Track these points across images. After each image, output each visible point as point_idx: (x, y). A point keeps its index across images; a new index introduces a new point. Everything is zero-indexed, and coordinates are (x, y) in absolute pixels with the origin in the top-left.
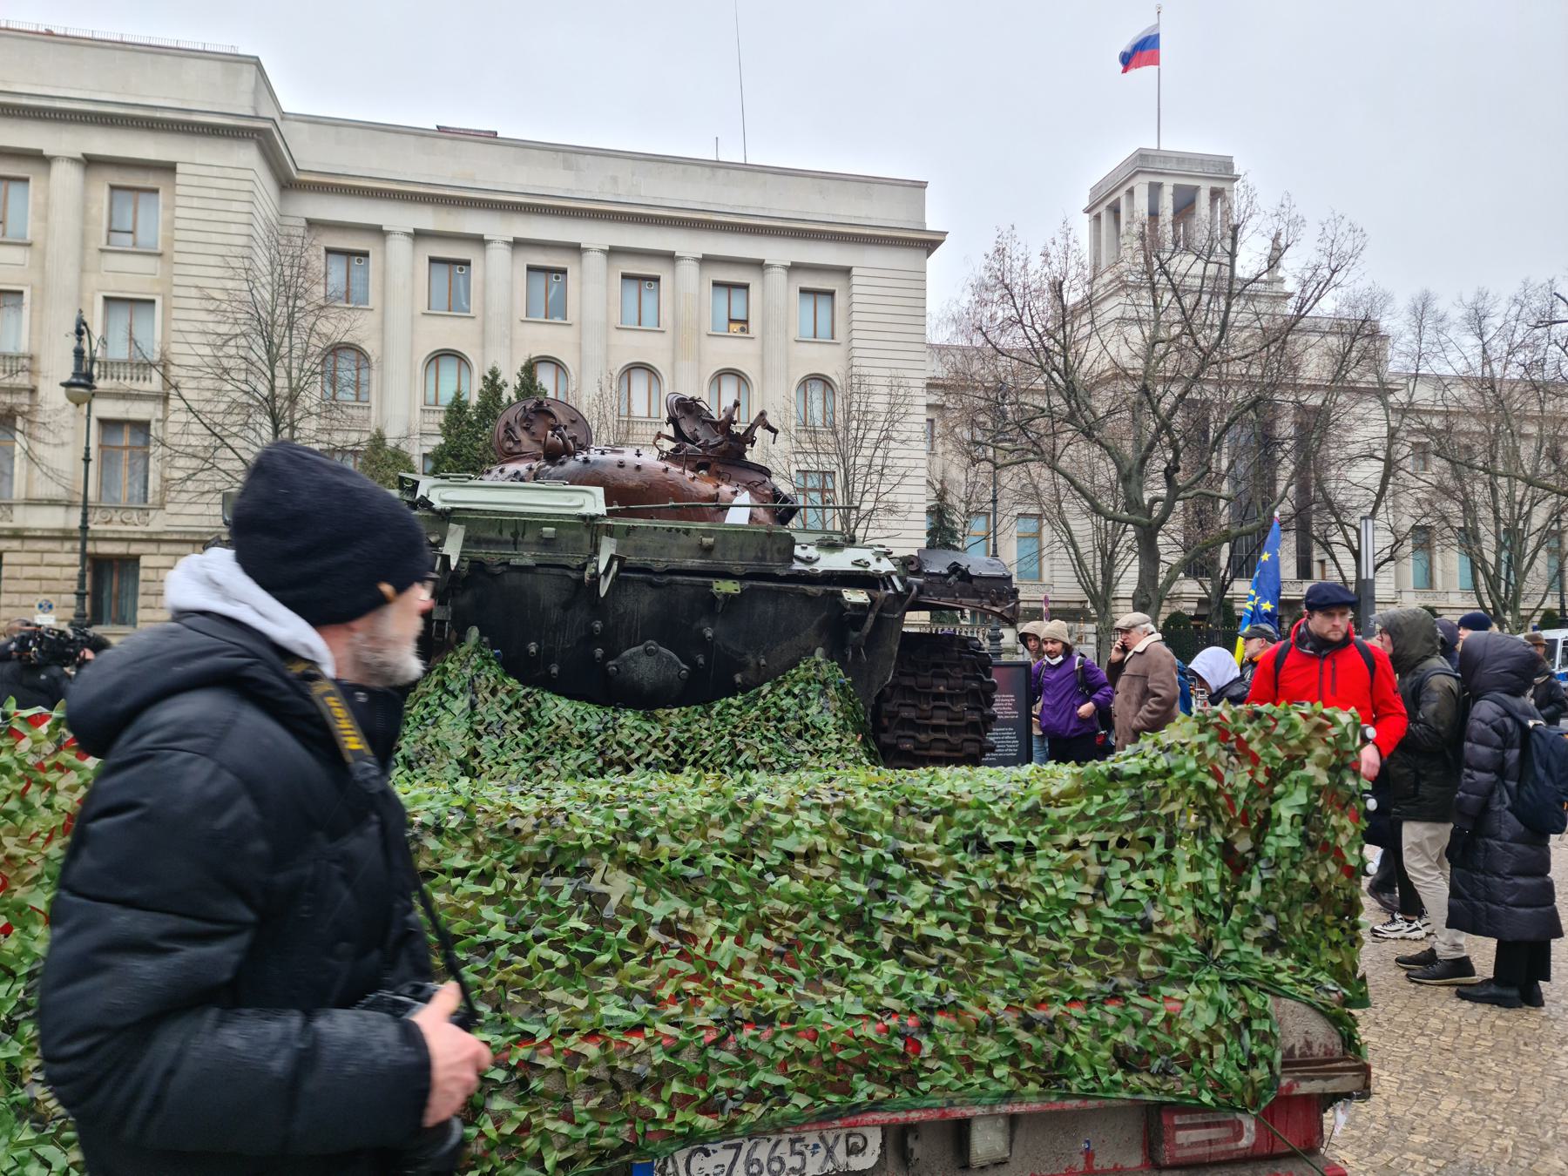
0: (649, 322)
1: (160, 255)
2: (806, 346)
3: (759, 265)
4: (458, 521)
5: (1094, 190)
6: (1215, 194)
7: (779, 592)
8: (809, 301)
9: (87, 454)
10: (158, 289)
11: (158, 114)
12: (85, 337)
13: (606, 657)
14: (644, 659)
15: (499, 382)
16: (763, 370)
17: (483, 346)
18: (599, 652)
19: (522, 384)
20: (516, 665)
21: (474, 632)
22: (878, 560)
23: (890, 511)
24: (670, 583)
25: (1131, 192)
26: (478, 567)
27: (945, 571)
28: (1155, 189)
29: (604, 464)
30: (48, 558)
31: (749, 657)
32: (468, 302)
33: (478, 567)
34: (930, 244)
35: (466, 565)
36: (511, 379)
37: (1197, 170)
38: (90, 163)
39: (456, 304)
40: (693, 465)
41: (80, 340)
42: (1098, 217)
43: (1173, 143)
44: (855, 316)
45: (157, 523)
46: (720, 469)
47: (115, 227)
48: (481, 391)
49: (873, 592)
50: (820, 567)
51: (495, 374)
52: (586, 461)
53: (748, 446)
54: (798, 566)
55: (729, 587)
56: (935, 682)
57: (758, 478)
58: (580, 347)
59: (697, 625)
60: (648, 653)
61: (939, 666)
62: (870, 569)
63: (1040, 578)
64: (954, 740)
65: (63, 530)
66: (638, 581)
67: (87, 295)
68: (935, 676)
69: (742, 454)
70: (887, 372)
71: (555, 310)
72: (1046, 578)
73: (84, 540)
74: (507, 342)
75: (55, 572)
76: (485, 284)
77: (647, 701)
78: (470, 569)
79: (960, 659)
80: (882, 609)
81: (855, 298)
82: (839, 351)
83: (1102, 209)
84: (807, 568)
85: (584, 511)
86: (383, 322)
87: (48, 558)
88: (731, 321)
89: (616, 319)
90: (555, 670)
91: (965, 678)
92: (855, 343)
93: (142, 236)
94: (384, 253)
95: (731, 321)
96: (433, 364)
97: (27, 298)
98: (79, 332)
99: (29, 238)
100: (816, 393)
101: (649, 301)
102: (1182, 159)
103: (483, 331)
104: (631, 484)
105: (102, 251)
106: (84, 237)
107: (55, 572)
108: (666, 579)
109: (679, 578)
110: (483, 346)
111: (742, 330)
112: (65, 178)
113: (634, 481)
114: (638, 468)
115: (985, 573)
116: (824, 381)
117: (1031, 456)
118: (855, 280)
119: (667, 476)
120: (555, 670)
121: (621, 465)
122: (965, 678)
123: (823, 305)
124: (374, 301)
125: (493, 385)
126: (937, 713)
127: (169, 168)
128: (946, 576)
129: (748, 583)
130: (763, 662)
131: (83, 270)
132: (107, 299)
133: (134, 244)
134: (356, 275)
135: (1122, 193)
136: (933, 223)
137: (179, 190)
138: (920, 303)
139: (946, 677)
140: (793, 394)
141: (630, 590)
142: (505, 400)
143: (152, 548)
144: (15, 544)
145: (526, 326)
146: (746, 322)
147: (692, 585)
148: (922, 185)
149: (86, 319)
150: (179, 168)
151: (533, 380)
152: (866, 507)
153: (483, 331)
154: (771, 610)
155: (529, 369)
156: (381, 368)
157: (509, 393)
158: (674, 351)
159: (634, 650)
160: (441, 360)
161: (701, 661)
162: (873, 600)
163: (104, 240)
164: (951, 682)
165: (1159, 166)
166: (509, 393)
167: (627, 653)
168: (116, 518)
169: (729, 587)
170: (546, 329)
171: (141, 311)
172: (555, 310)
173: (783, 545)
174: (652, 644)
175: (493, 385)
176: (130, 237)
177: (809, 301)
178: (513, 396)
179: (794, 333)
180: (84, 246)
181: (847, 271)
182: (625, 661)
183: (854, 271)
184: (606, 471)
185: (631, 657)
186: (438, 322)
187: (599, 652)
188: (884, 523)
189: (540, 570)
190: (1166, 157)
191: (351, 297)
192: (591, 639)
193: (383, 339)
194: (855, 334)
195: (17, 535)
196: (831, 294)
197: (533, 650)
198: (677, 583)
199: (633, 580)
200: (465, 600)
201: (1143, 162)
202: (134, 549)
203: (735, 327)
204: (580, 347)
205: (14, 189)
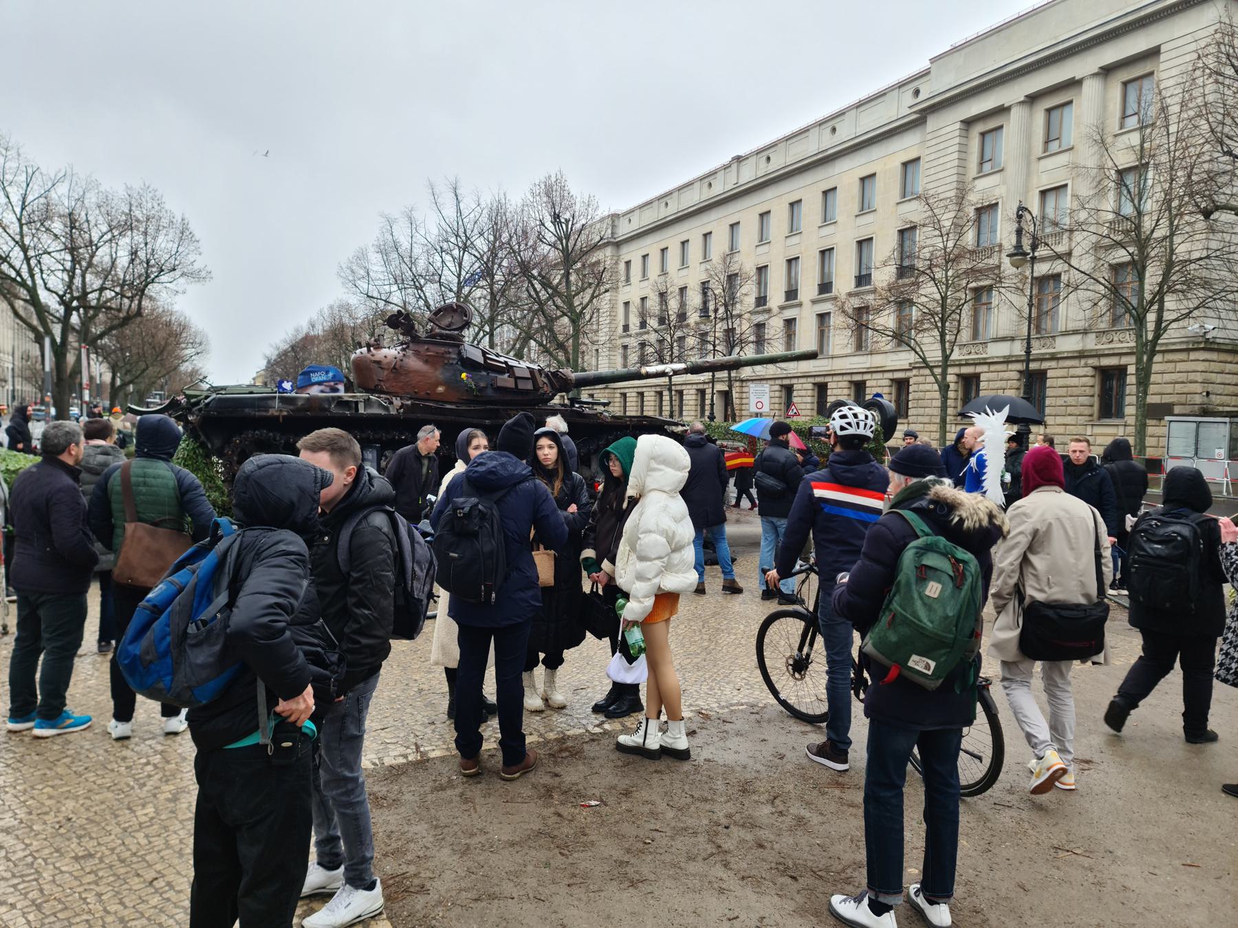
11: (1142, 13)
30: (1072, 372)
38: (1107, 71)
65: (1079, 352)
73: (1028, 361)
75: (1074, 381)
87: (1072, 372)
98: (1020, 217)
107: (1074, 381)
112: (1091, 89)
127: (1154, 53)
137: (1162, 67)
144: (1053, 364)
150: (1163, 49)
163: (1117, 127)
176: (1136, 117)
195: (1053, 357)
205: (1066, 110)
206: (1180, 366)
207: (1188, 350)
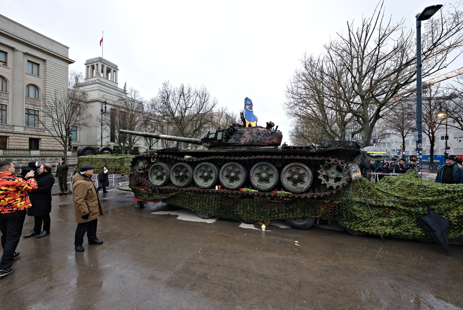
3: (13, 49)
5: (87, 61)
6: (114, 71)
8: (30, 65)
16: (13, 78)
25: (97, 64)
28: (103, 66)
34: (70, 62)
37: (111, 66)
42: (88, 67)
43: (105, 57)
63: (76, 140)
70: (54, 88)
72: (78, 140)
83: (89, 65)
102: (108, 62)
116: (36, 87)
118: (47, 64)
123: (35, 67)
135: (95, 64)
136: (71, 57)
146: (6, 63)
148: (68, 48)
165: (103, 61)
179: (25, 71)
181: (44, 61)
183: (47, 61)
190: (105, 61)
196: (38, 65)
201: (100, 60)
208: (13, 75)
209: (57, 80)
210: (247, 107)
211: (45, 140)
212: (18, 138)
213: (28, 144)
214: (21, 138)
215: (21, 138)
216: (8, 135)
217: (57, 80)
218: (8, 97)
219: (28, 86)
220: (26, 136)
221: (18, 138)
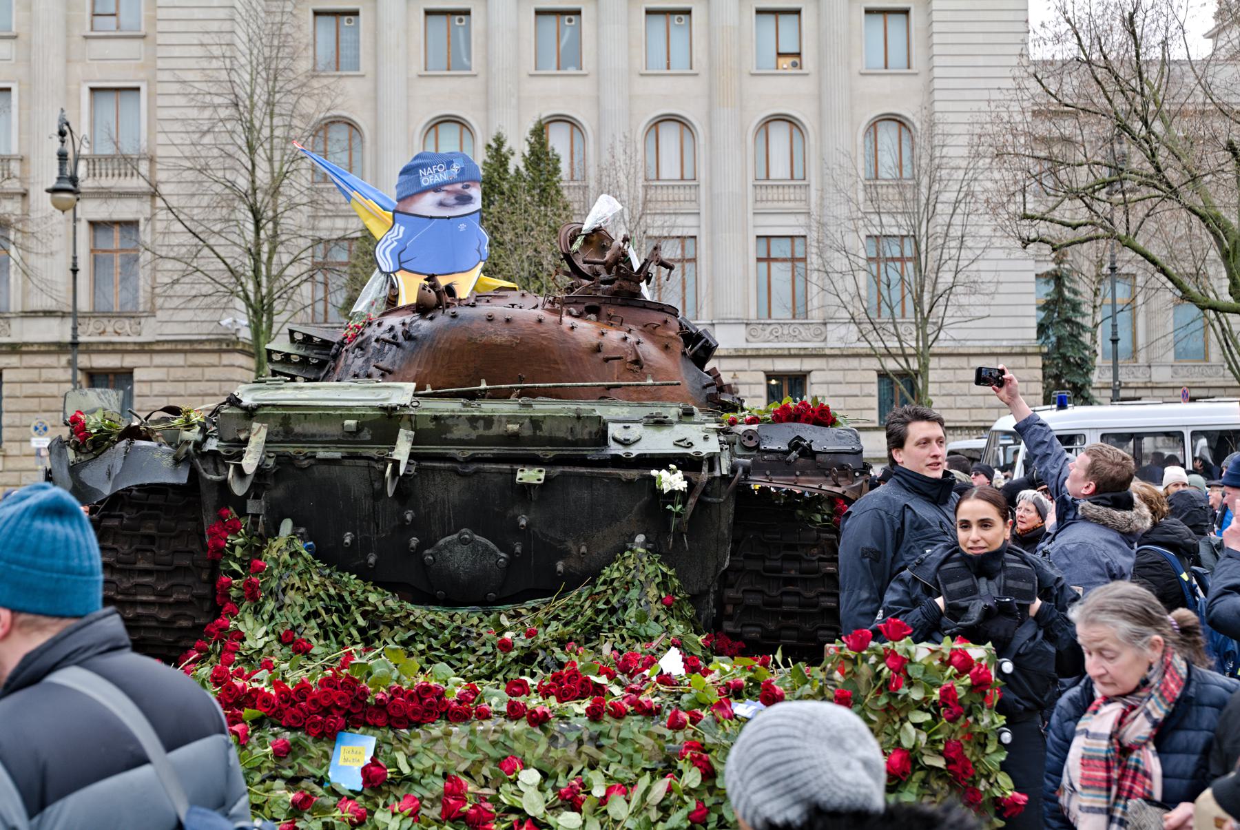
0: (679, 64)
1: (144, 37)
2: (874, 79)
4: (264, 419)
7: (592, 477)
9: (75, 264)
10: (142, 75)
12: (68, 137)
13: (421, 547)
14: (458, 548)
15: (504, 150)
16: (820, 114)
17: (487, 108)
18: (414, 541)
19: (533, 153)
20: (328, 554)
21: (287, 527)
22: (706, 438)
23: (973, 287)
24: (477, 472)
26: (285, 461)
27: (785, 448)
29: (472, 319)
30: (46, 374)
31: (570, 544)
32: (469, 58)
33: (285, 461)
35: (271, 462)
36: (518, 148)
39: (455, 61)
40: (582, 308)
41: (63, 142)
44: (936, 39)
45: (149, 332)
46: (612, 311)
47: (98, 11)
48: (485, 163)
49: (692, 475)
50: (635, 451)
51: (500, 141)
52: (454, 316)
53: (643, 284)
54: (615, 449)
55: (530, 475)
56: (787, 565)
57: (657, 318)
58: (598, 101)
59: (510, 513)
60: (463, 542)
61: (792, 547)
62: (690, 451)
64: (807, 627)
66: (445, 470)
67: (73, 87)
68: (785, 558)
69: (638, 294)
71: (569, 59)
74: (514, 101)
76: (487, 34)
77: (451, 594)
78: (277, 463)
79: (819, 538)
80: (704, 493)
81: (936, 16)
82: (917, 83)
84: (620, 450)
85: (386, 404)
86: (376, 89)
87: (46, 374)
88: (779, 55)
89: (639, 64)
90: (372, 560)
91: (820, 560)
92: (937, 72)
93: (124, 18)
94: (375, 9)
95: (779, 55)
96: (433, 131)
97: (14, 92)
98: (62, 134)
99: (14, 31)
100: (888, 135)
101: (678, 37)
103: (487, 92)
104: (499, 340)
105: (86, 37)
106: (68, 23)
108: (473, 467)
109: (487, 466)
110: (487, 108)
111: (794, 65)
113: (502, 336)
114: (508, 321)
115: (829, 448)
117: (1101, 231)
119: (541, 329)
120: (372, 560)
121: (490, 319)
122: (820, 560)
124: (365, 64)
125: (498, 156)
126: (785, 599)
128: (787, 453)
129: (559, 470)
130: (583, 549)
131: (68, 61)
132: (93, 90)
133: (118, 28)
134: (346, 37)
138: (1021, 16)
139: (798, 559)
140: (860, 138)
141: (438, 479)
142: (512, 171)
143: (143, 359)
144: (14, 360)
145: (534, 79)
146: (799, 55)
147: (500, 473)
149: (68, 119)
151: (543, 145)
152: (946, 278)
153: (487, 92)
154: (586, 495)
155: (539, 132)
156: (375, 142)
157: (516, 163)
158: (710, 97)
159: (448, 538)
160: (441, 127)
161: (518, 549)
162: (691, 486)
163: (88, 27)
164: (805, 565)
166: (516, 163)
167: (441, 542)
168: (110, 329)
169: (530, 475)
170: (558, 83)
171: (127, 98)
172: (569, 59)
173: (594, 428)
174: (466, 533)
175: (498, 156)
176: (113, 18)
177: (878, 20)
178: (521, 165)
179: (858, 65)
180: (68, 35)
182: (440, 550)
184: (475, 325)
185: (445, 546)
186: (437, 83)
187: (414, 541)
188: (963, 300)
189: (347, 462)
191: (342, 61)
192: (404, 529)
193: (376, 110)
194: (937, 61)
195: (14, 349)
197: (348, 540)
198: (485, 471)
199: (440, 469)
200: (279, 492)
202: (128, 361)
203: (785, 63)
204: (598, 101)
206: (210, 373)
207: (220, 351)
208: (820, 98)
209: (981, 61)
210: (426, 205)
211: (829, 376)
212: (838, 376)
213: (875, 402)
214: (850, 377)
215: (850, 377)
216: (806, 365)
217: (981, 61)
218: (807, 201)
219: (874, 125)
220: (866, 363)
221: (838, 376)
